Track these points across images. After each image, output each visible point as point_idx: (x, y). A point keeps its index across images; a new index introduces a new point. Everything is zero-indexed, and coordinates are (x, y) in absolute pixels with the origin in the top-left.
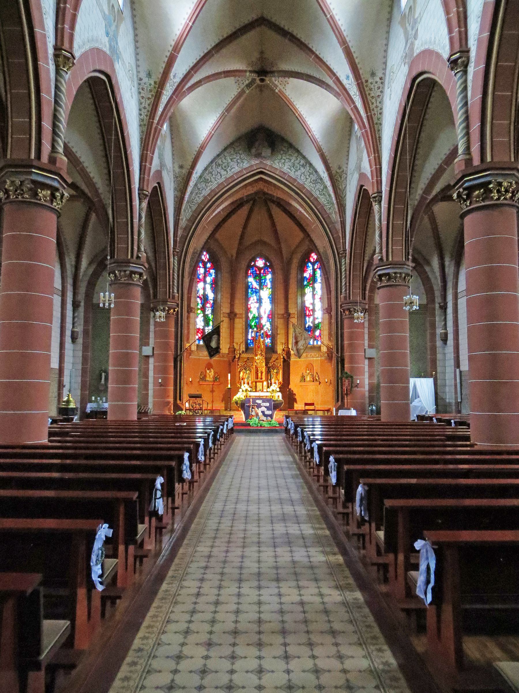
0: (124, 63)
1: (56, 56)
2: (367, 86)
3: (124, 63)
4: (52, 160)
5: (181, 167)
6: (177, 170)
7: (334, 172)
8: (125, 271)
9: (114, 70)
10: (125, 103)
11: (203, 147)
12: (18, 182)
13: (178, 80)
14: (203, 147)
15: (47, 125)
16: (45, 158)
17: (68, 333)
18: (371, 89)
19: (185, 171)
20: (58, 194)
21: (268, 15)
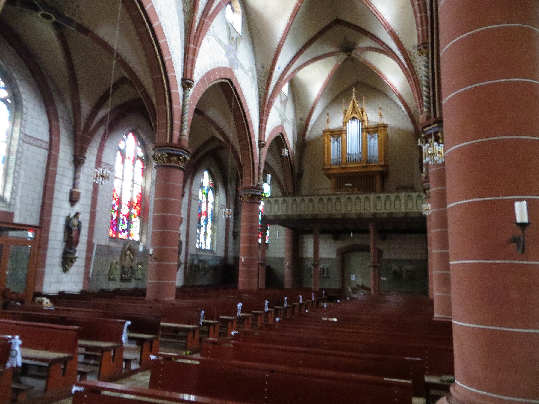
0: (243, 68)
1: (182, 83)
2: (411, 56)
3: (243, 68)
4: (180, 140)
5: (301, 119)
6: (299, 121)
7: (412, 111)
8: (247, 195)
9: (233, 75)
10: (244, 93)
11: (315, 104)
12: (159, 155)
13: (282, 69)
14: (315, 104)
15: (177, 122)
16: (175, 141)
17: (231, 233)
18: (414, 58)
19: (304, 122)
20: (181, 158)
21: (341, 17)
